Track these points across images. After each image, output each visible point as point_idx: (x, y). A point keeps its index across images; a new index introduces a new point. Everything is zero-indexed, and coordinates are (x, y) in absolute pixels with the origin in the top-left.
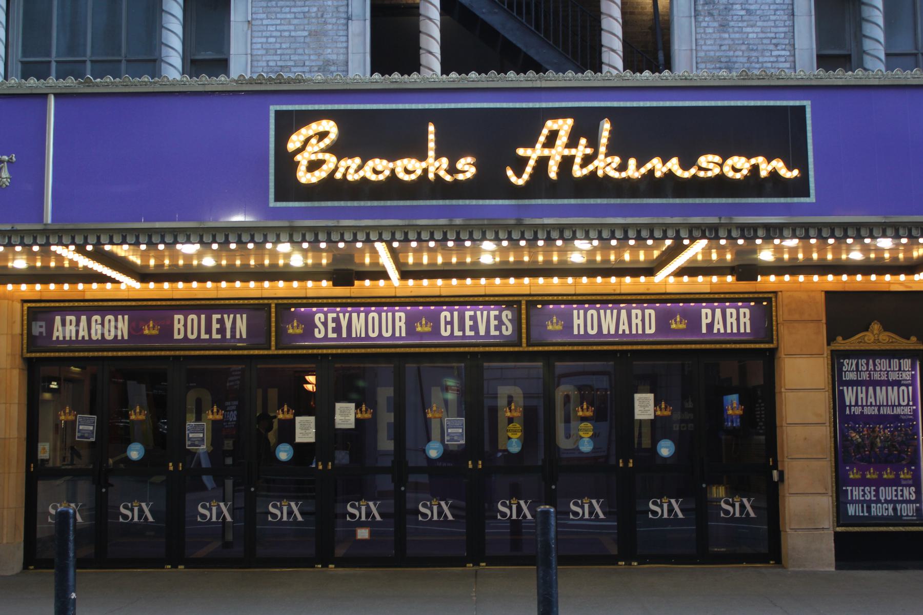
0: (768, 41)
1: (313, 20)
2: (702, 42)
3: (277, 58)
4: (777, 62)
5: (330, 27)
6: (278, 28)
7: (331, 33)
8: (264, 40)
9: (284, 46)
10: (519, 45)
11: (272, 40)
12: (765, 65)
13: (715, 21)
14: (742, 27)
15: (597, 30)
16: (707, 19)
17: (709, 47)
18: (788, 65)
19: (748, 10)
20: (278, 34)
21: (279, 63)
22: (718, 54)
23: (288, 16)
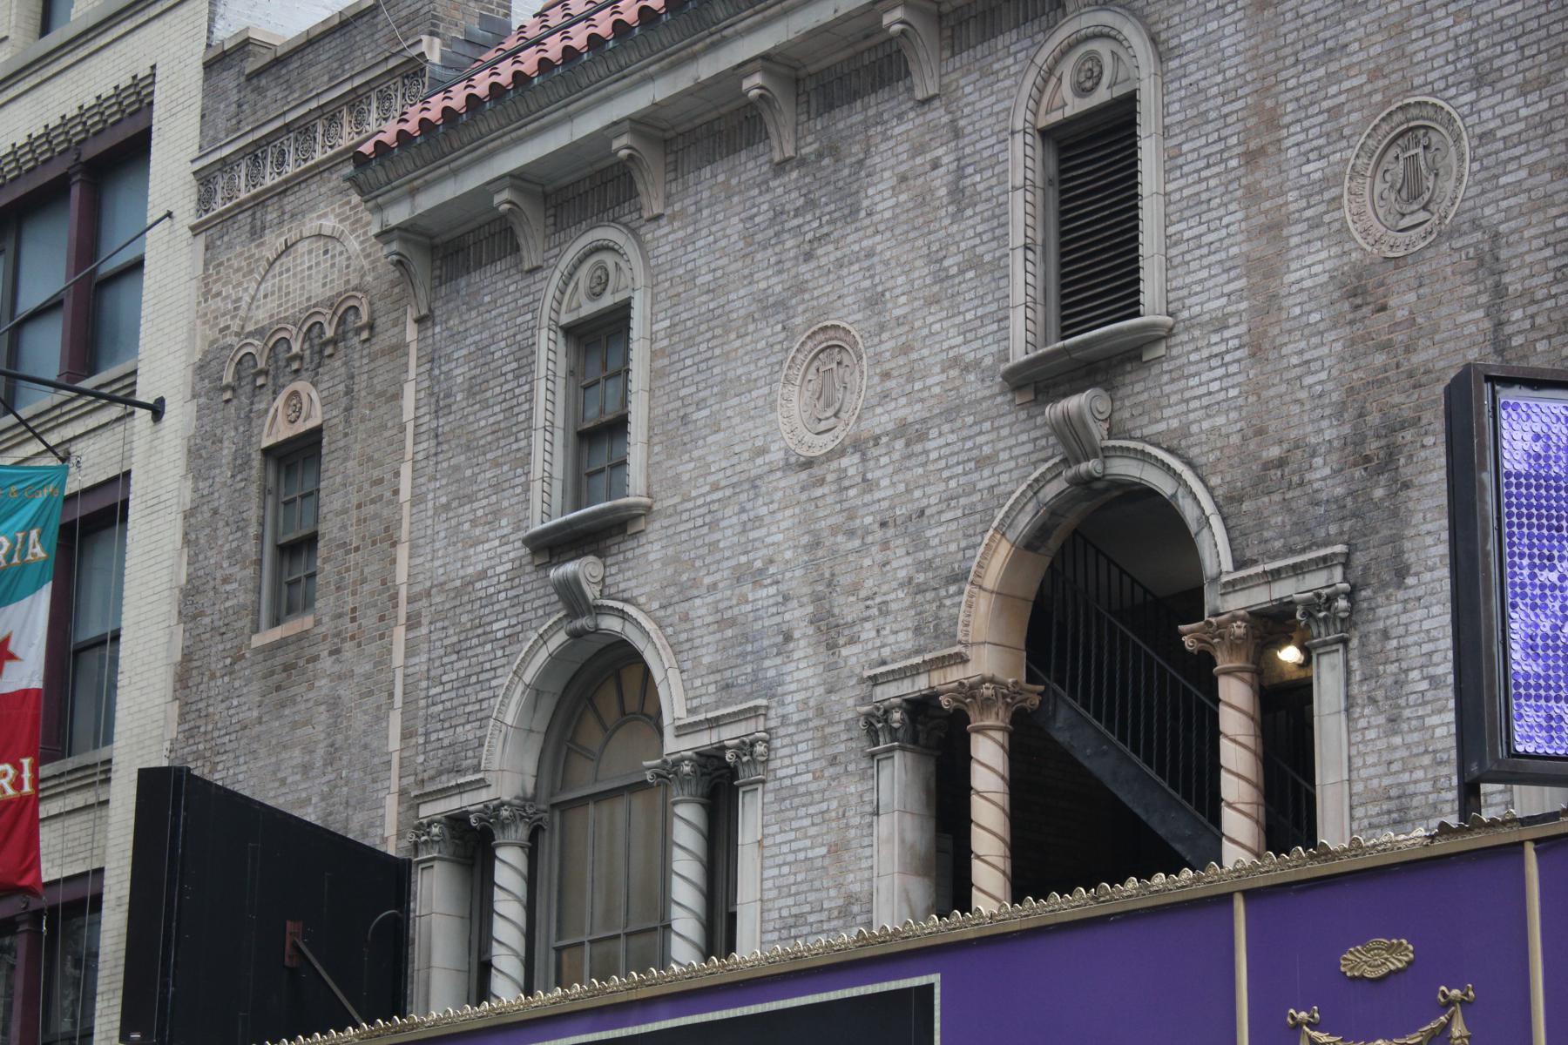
1: (834, 825)
2: (1358, 762)
3: (790, 901)
5: (852, 832)
6: (795, 846)
7: (854, 844)
8: (775, 872)
9: (800, 878)
10: (1138, 811)
11: (785, 870)
14: (1422, 717)
15: (1214, 767)
16: (1367, 711)
17: (1371, 774)
20: (790, 858)
21: (795, 911)
22: (1386, 781)
23: (807, 822)
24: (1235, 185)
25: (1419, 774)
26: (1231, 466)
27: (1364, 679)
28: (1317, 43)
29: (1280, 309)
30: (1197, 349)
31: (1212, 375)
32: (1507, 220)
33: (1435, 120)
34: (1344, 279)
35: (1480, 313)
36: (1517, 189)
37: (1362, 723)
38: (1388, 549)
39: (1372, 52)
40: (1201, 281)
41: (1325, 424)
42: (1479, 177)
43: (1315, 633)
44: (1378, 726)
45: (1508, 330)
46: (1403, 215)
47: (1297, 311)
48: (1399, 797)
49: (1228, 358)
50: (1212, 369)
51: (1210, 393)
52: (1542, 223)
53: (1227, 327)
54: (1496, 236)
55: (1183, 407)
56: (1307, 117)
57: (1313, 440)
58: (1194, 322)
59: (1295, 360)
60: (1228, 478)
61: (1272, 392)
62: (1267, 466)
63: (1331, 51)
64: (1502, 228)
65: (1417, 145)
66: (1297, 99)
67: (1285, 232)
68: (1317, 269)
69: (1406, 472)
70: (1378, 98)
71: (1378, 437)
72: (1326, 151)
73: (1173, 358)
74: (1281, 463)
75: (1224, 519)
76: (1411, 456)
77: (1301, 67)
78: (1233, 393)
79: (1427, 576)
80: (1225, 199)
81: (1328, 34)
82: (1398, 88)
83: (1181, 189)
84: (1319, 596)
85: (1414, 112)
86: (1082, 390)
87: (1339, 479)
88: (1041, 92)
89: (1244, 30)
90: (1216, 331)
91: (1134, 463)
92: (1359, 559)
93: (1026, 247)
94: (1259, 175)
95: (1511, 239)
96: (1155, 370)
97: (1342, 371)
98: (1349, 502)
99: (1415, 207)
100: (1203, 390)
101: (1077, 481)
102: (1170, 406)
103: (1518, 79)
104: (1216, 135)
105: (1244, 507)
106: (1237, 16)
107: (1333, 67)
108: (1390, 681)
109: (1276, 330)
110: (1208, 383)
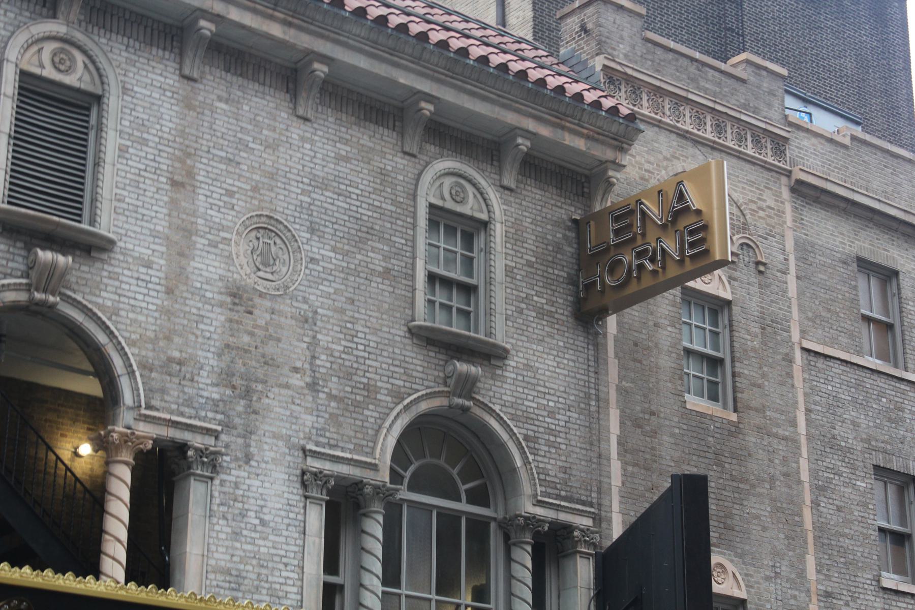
0: (277, 559)
2: (213, 548)
4: (286, 584)
12: (274, 586)
13: (228, 525)
14: (254, 539)
16: (221, 522)
17: (220, 557)
18: (295, 590)
19: (262, 520)
22: (228, 565)
24: (164, 193)
25: (250, 568)
26: (147, 349)
27: (222, 504)
28: (222, 150)
29: (187, 277)
30: (129, 269)
31: (138, 289)
32: (321, 307)
33: (284, 234)
34: (229, 285)
35: (305, 345)
36: (328, 296)
37: (217, 528)
38: (240, 441)
39: (254, 177)
40: (134, 232)
41: (210, 355)
42: (309, 277)
43: (195, 467)
44: (227, 533)
45: (318, 362)
46: (259, 270)
47: (199, 285)
48: (237, 576)
49: (150, 285)
50: (137, 285)
51: (135, 299)
52: (339, 320)
53: (151, 268)
54: (316, 312)
55: (117, 298)
56: (212, 185)
57: (202, 360)
58: (129, 253)
59: (194, 311)
60: (144, 353)
61: (177, 320)
62: (170, 360)
63: (230, 160)
64: (319, 310)
65: (270, 238)
66: (208, 172)
67: (194, 238)
68: (213, 270)
69: (256, 406)
70: (256, 202)
71: (242, 378)
72: (222, 210)
73: (112, 265)
74: (180, 363)
75: (141, 376)
76: (260, 399)
77: (211, 156)
78: (150, 307)
79: (263, 465)
80: (156, 196)
81: (230, 150)
82: (267, 205)
83: (126, 172)
84: (207, 449)
85: (273, 222)
86: (64, 255)
87: (215, 389)
88: (28, 47)
89: (177, 112)
90: (143, 266)
91: (77, 310)
92: (223, 437)
93: (10, 136)
94: (178, 195)
95: (324, 318)
96: (98, 265)
97: (223, 333)
98: (221, 404)
99: (268, 270)
100: (132, 295)
101: (43, 304)
102: (106, 291)
103: (333, 243)
104: (152, 157)
105: (154, 375)
106: (173, 101)
107: (231, 169)
108: (237, 512)
109: (185, 288)
110: (135, 292)
